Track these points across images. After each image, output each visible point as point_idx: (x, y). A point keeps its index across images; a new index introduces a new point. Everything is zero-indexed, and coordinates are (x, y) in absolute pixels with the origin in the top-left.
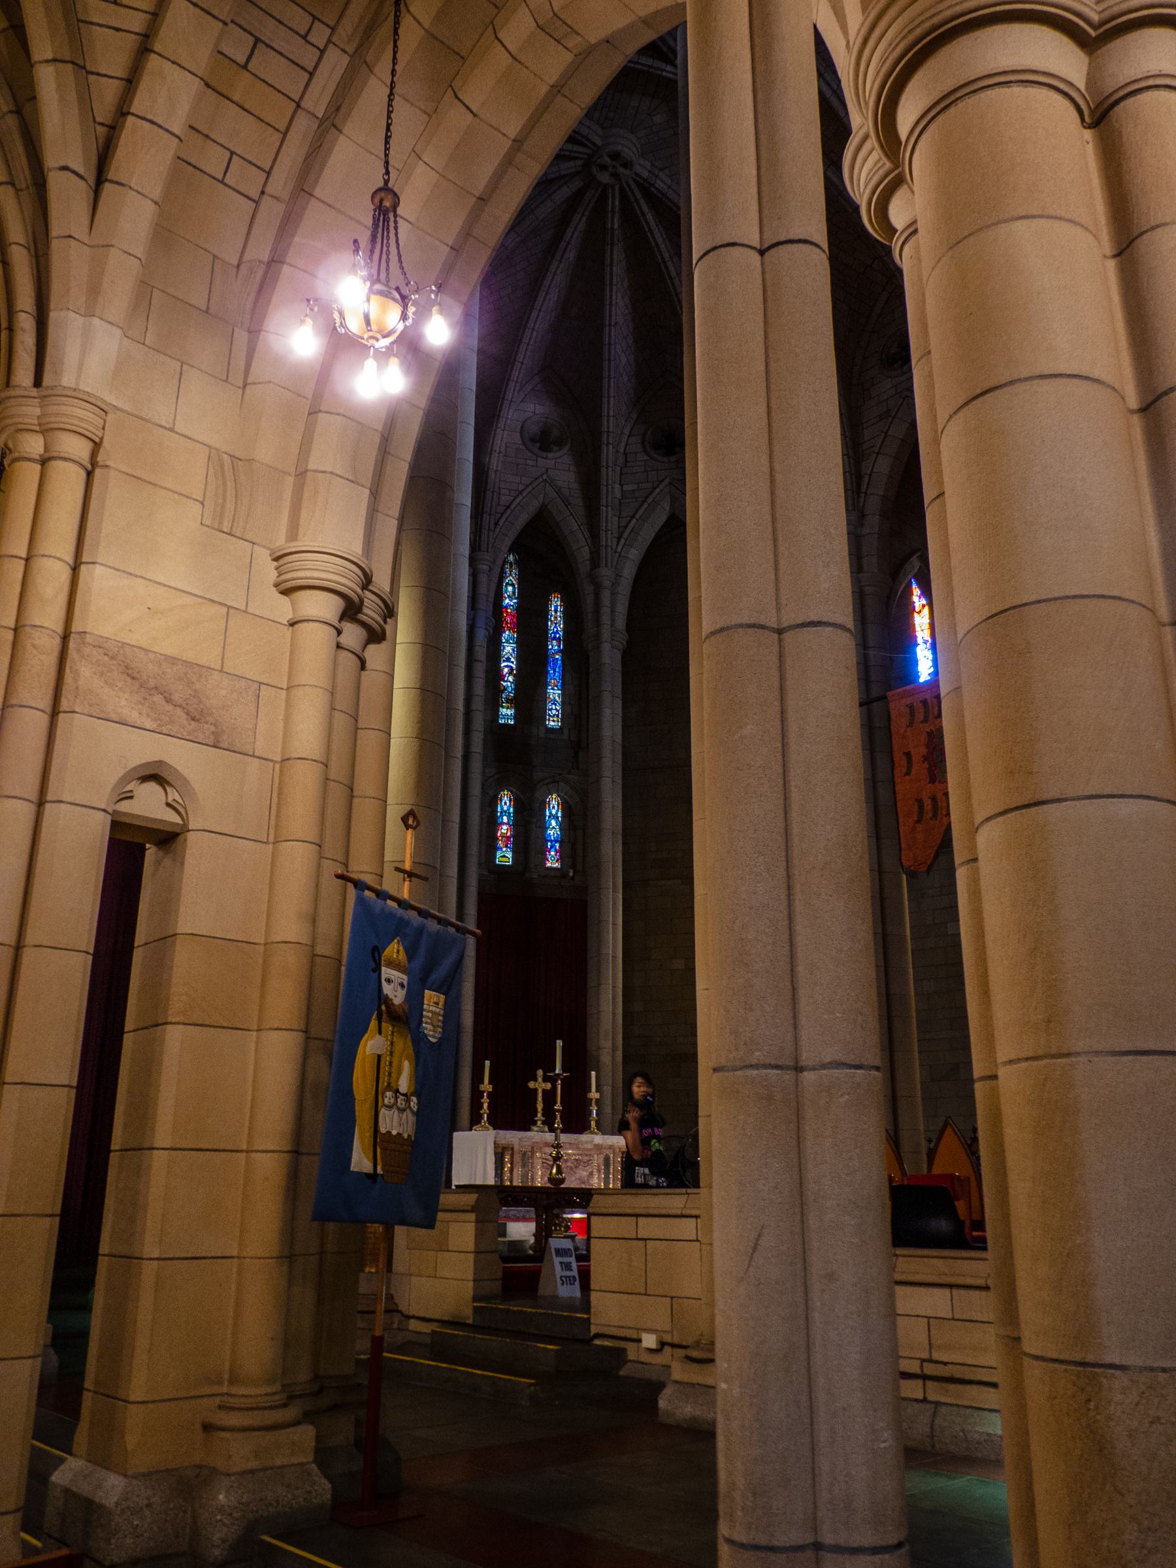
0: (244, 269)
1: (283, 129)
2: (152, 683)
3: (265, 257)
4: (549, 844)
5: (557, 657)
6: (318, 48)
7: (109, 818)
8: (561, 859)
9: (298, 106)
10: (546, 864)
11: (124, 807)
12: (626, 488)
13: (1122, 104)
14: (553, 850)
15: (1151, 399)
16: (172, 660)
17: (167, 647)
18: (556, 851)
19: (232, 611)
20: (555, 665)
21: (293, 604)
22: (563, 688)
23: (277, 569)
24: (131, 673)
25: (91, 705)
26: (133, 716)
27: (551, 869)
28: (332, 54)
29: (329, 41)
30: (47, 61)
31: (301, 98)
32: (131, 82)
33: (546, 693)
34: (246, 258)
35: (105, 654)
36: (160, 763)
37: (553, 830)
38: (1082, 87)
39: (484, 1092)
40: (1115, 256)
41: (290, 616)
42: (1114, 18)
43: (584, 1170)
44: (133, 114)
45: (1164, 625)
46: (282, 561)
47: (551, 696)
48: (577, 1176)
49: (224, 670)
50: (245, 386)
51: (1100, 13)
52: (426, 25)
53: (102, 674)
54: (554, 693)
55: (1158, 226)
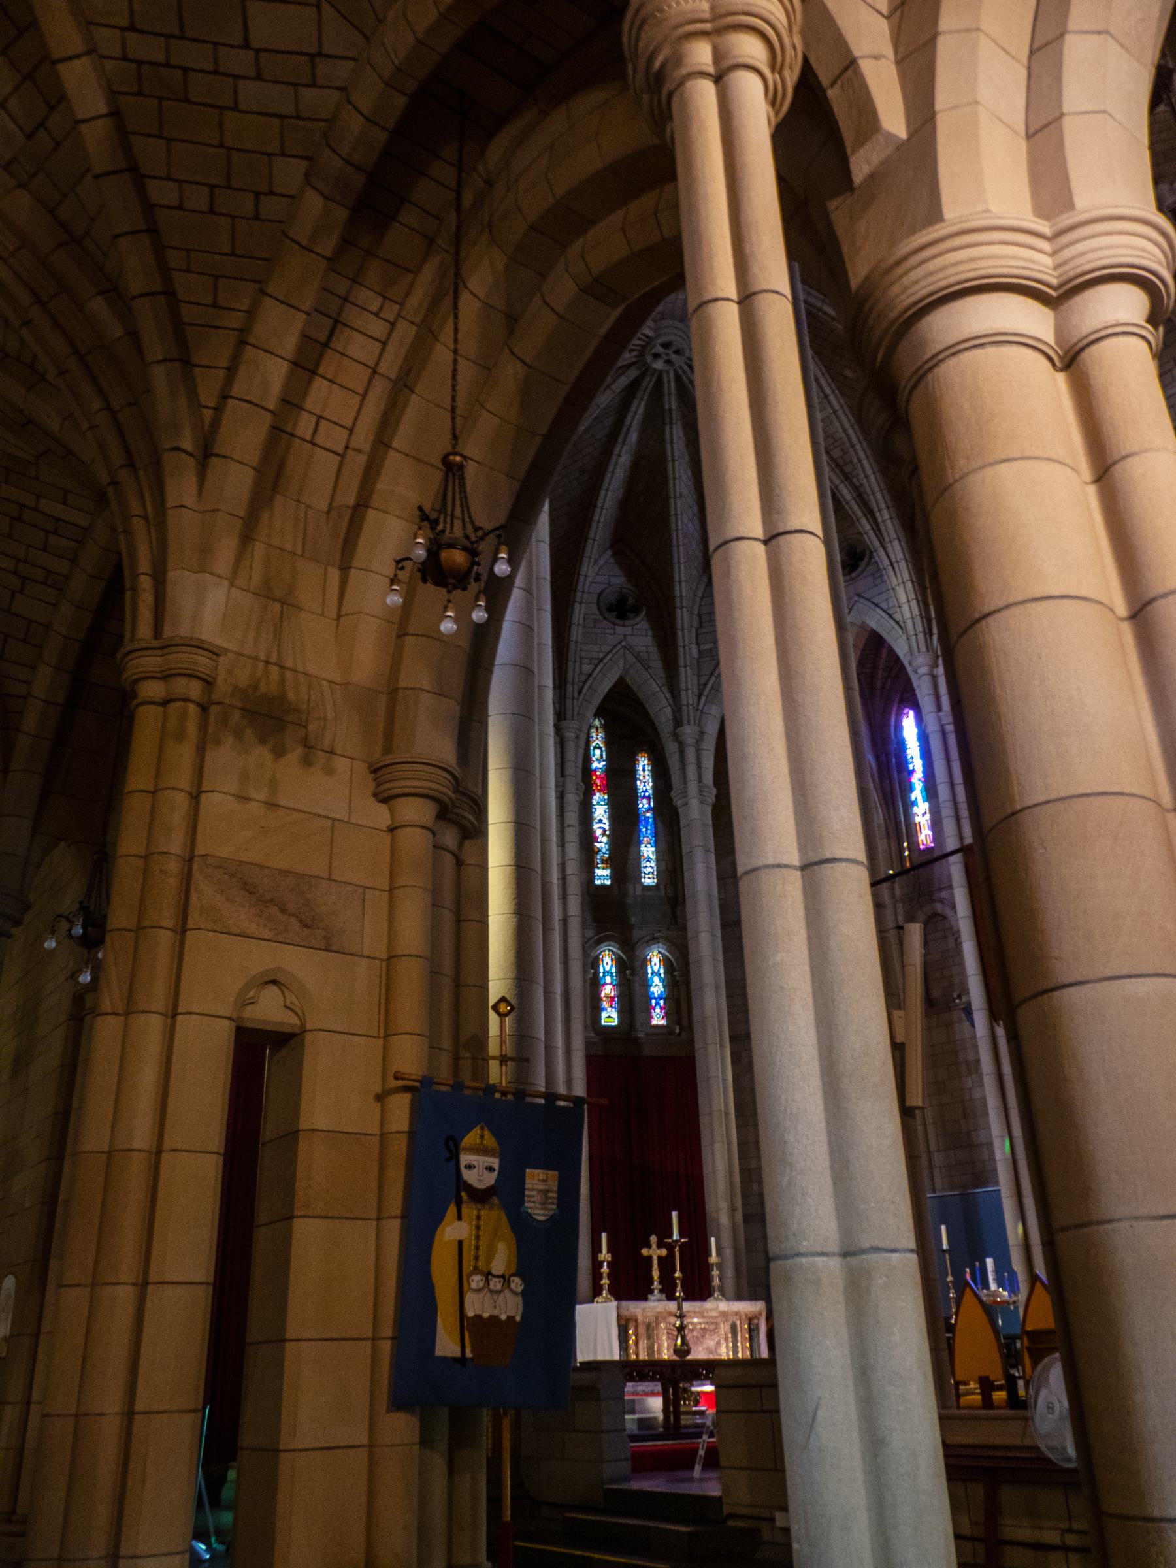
0: (334, 513)
1: (361, 390)
2: (268, 896)
3: (351, 501)
4: (653, 1002)
5: (648, 815)
6: (388, 321)
7: (233, 1025)
8: (666, 1016)
9: (375, 372)
10: (651, 1022)
11: (248, 1012)
12: (703, 647)
13: (1087, 351)
14: (657, 1007)
15: (1137, 609)
16: (285, 873)
18: (661, 1008)
19: (337, 823)
20: (647, 822)
21: (391, 811)
22: (656, 845)
23: (375, 780)
24: (248, 888)
26: (252, 928)
27: (657, 1026)
28: (402, 326)
29: (399, 315)
30: (158, 362)
31: (377, 363)
32: (231, 370)
33: (639, 851)
35: (225, 874)
37: (657, 988)
38: (1052, 342)
41: (389, 822)
42: (1070, 280)
43: (711, 1340)
45: (1168, 811)
47: (646, 855)
48: (705, 1346)
49: (332, 878)
51: (1057, 277)
52: (482, 295)
54: (648, 851)
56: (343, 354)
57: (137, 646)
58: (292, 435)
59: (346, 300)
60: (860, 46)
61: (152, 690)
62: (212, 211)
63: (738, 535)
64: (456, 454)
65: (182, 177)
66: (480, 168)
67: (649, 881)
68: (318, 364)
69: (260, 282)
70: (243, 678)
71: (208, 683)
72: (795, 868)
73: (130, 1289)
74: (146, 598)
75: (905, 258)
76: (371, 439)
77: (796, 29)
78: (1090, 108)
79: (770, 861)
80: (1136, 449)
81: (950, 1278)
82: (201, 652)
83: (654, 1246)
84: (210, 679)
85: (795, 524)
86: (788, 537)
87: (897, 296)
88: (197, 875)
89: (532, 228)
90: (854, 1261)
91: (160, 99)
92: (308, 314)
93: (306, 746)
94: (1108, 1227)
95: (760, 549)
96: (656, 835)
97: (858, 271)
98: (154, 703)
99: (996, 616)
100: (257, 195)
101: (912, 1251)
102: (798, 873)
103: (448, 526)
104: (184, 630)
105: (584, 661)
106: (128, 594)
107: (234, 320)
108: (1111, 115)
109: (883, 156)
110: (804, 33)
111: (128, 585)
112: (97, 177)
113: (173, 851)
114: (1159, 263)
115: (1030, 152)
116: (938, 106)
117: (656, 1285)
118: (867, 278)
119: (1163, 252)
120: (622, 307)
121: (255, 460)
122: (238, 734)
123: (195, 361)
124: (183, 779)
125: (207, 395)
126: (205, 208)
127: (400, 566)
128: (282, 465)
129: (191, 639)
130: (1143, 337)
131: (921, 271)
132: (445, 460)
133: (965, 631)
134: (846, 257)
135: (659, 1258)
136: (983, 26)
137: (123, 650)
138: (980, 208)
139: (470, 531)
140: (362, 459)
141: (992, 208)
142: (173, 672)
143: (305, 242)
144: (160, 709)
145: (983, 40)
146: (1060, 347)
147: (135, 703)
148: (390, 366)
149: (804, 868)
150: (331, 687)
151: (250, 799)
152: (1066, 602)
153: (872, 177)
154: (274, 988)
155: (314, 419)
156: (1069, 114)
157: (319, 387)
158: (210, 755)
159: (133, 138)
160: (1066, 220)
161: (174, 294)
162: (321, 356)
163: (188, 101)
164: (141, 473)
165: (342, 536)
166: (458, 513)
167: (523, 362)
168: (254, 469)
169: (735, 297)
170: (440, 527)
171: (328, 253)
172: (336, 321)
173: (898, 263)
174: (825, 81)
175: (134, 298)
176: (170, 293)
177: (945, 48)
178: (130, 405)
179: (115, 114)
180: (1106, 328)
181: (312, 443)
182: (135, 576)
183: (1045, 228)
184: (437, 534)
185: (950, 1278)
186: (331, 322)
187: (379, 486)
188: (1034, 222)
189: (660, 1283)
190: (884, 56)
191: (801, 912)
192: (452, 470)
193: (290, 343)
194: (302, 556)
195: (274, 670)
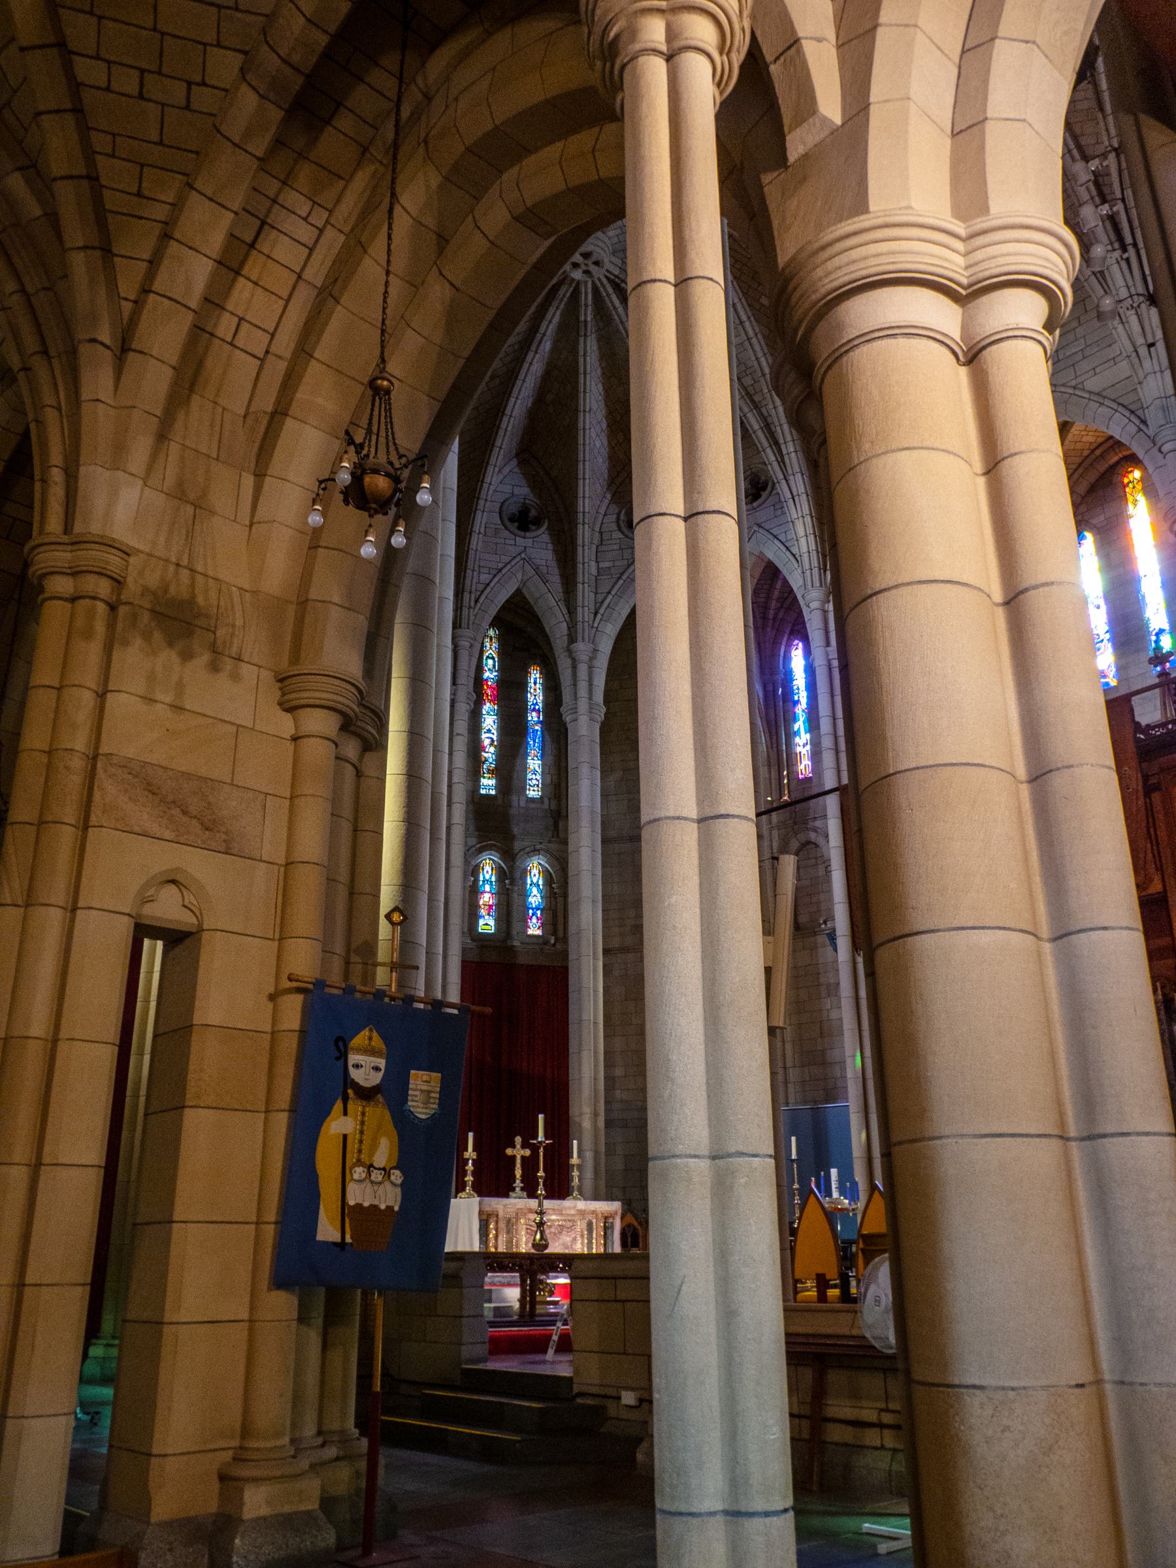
0: (249, 421)
1: (285, 295)
2: (170, 798)
3: (270, 409)
4: (531, 911)
5: (537, 728)
6: (317, 228)
7: (133, 921)
9: (300, 277)
10: (527, 931)
12: (602, 565)
13: (988, 349)
14: (534, 917)
15: (1012, 596)
16: (187, 776)
18: (538, 919)
19: (241, 729)
21: (296, 721)
23: (281, 689)
24: (151, 789)
25: (117, 820)
26: (155, 829)
28: (330, 233)
29: (327, 222)
30: (79, 248)
32: (154, 263)
36: (178, 869)
37: (535, 898)
40: (985, 474)
41: (293, 732)
42: (980, 282)
44: (154, 292)
45: (1022, 783)
46: (287, 682)
47: (531, 767)
51: (968, 277)
52: (414, 212)
53: (126, 791)
54: (534, 763)
55: (1016, 454)
56: (268, 257)
57: (47, 540)
58: (212, 335)
59: (274, 201)
60: (803, 28)
61: (61, 585)
62: (141, 96)
63: (662, 511)
64: (383, 379)
65: (113, 58)
66: (420, 81)
67: (533, 793)
68: (242, 263)
69: (188, 175)
70: (153, 580)
71: (118, 583)
72: (692, 820)
73: (24, 1169)
74: (57, 492)
75: (830, 244)
76: (292, 346)
77: (746, 13)
78: (1012, 116)
79: (671, 813)
80: (1023, 448)
81: (796, 1186)
82: (113, 551)
83: (518, 1146)
84: (120, 578)
85: (712, 505)
86: (706, 516)
87: (820, 279)
89: (468, 149)
92: (236, 213)
94: (938, 1142)
95: (680, 525)
96: (543, 748)
97: (786, 250)
98: (61, 598)
99: (886, 594)
100: (189, 84)
101: (770, 1156)
102: (696, 825)
103: (373, 450)
104: (95, 528)
105: (482, 570)
106: (38, 486)
107: (160, 212)
108: (1030, 125)
109: (818, 139)
110: (753, 17)
111: (37, 475)
113: (77, 748)
114: (1060, 273)
115: (954, 151)
116: (872, 99)
118: (793, 258)
119: (1065, 263)
120: (553, 239)
121: (174, 361)
122: (147, 637)
123: (115, 250)
124: (89, 676)
125: (128, 287)
126: (136, 93)
127: (323, 486)
128: (200, 364)
129: (102, 537)
130: (1040, 342)
131: (844, 258)
132: (372, 383)
134: (776, 233)
135: (523, 1158)
136: (920, 23)
137: (32, 543)
138: (904, 204)
139: (394, 458)
140: (282, 366)
141: (913, 205)
143: (237, 140)
144: (70, 605)
145: (920, 37)
147: (41, 597)
148: (317, 272)
149: (701, 821)
150: (241, 594)
151: (156, 701)
152: (949, 586)
153: (805, 157)
154: (173, 889)
155: (236, 320)
156: (991, 119)
158: (116, 655)
159: (61, 11)
160: (980, 224)
161: (97, 179)
162: (247, 255)
164: (55, 362)
166: (383, 433)
167: (451, 284)
168: (174, 368)
169: (672, 280)
170: (365, 452)
171: (259, 153)
172: (264, 223)
173: (823, 248)
174: (769, 58)
175: (55, 179)
176: (93, 178)
177: (884, 39)
178: (44, 289)
180: (1007, 330)
181: (231, 344)
182: (46, 468)
183: (960, 229)
184: (362, 459)
185: (796, 1186)
186: (258, 223)
187: (298, 395)
188: (950, 222)
189: (522, 1181)
190: (825, 39)
191: (696, 861)
192: (377, 392)
193: (216, 241)
194: (217, 459)
195: (185, 573)
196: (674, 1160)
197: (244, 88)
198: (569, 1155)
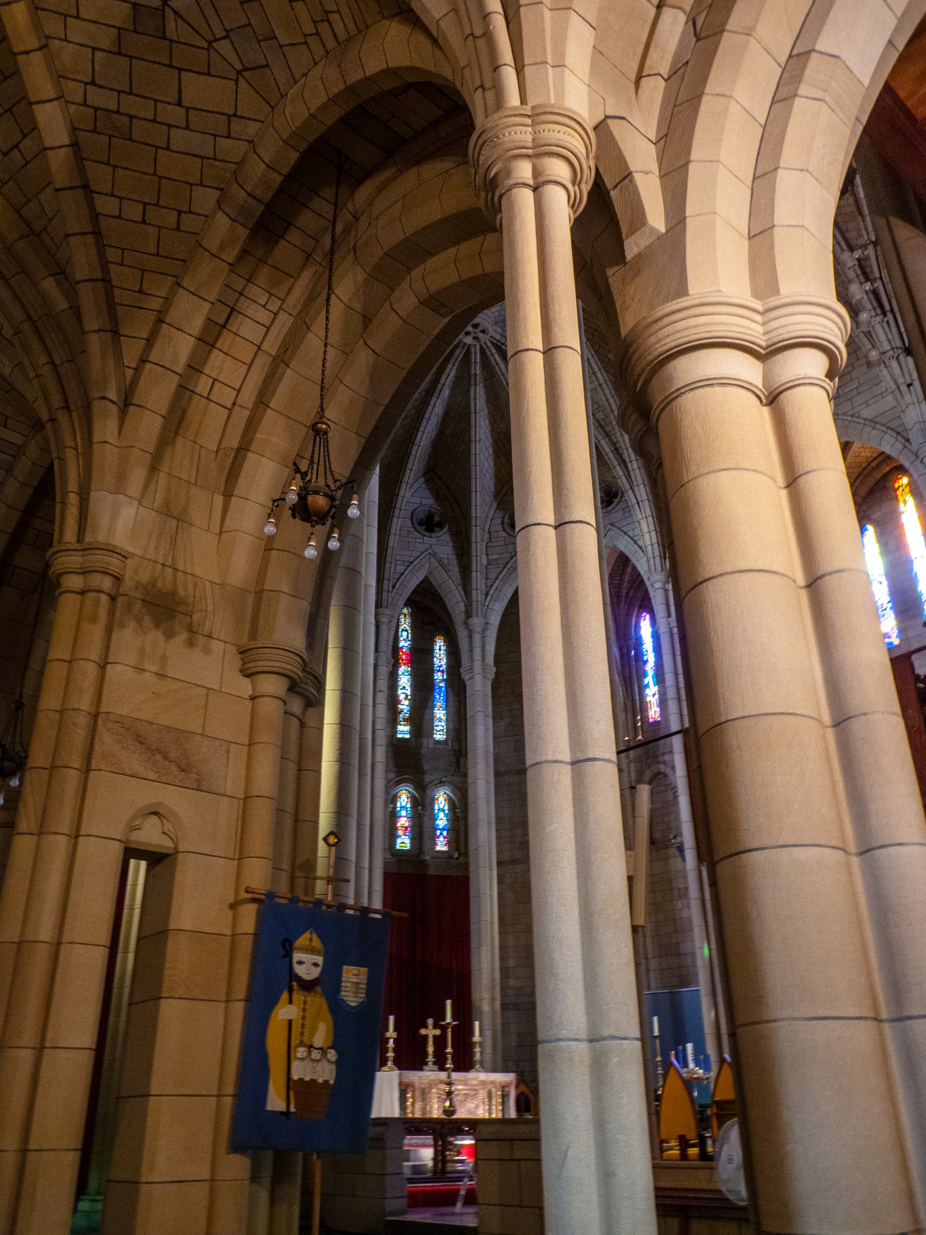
0: (221, 454)
1: (248, 362)
2: (155, 746)
3: (235, 445)
4: (438, 832)
5: (441, 685)
8: (448, 843)
9: (259, 348)
10: (434, 848)
12: (491, 557)
13: (784, 394)
15: (812, 580)
16: (169, 729)
17: (165, 720)
18: (445, 838)
20: (440, 691)
22: (447, 708)
23: (242, 659)
24: (140, 740)
25: (113, 764)
26: (141, 770)
27: (439, 852)
28: (282, 316)
29: (280, 307)
31: (262, 343)
32: (150, 341)
34: (223, 446)
36: (160, 803)
37: (442, 821)
38: (760, 386)
39: (389, 1038)
41: (250, 692)
42: (775, 344)
43: (472, 1103)
44: (150, 362)
46: (247, 654)
47: (438, 716)
48: (467, 1108)
49: (205, 734)
50: (220, 534)
51: (766, 341)
52: (345, 300)
54: (440, 713)
55: (809, 472)
57: (63, 548)
58: (193, 392)
59: (241, 294)
60: (634, 165)
61: (74, 582)
62: (144, 222)
63: (537, 522)
64: (323, 423)
66: (350, 205)
67: (439, 736)
69: (177, 277)
70: (144, 576)
71: (118, 579)
72: (567, 763)
74: (73, 511)
75: (660, 319)
76: (253, 399)
77: (591, 156)
78: (792, 223)
79: (550, 758)
80: (815, 467)
81: (659, 1059)
82: (115, 555)
84: (120, 577)
86: (572, 525)
87: (654, 345)
88: (101, 728)
89: (386, 254)
90: (597, 1045)
91: (110, 137)
92: (212, 303)
93: (190, 631)
95: (552, 532)
96: (447, 701)
97: (627, 323)
98: (73, 592)
99: (713, 581)
100: (179, 213)
101: (637, 1039)
102: (569, 767)
103: (314, 476)
104: (101, 538)
105: (398, 562)
106: (58, 506)
107: (155, 304)
108: (807, 229)
109: (648, 242)
110: (597, 158)
111: (58, 499)
112: (57, 190)
114: (836, 336)
115: (751, 249)
116: (687, 214)
117: (430, 1058)
118: (633, 329)
119: (839, 328)
120: (449, 318)
122: (139, 621)
123: (122, 331)
124: (94, 652)
125: (130, 358)
126: (140, 219)
127: (276, 504)
128: (184, 412)
129: (106, 545)
130: (823, 388)
131: (671, 329)
132: (314, 427)
133: (692, 589)
134: (619, 311)
135: (435, 1037)
136: (721, 160)
138: (715, 288)
139: (330, 482)
141: (722, 289)
142: (90, 569)
143: (214, 251)
144: (79, 597)
145: (721, 169)
146: (766, 390)
147: (59, 591)
148: (272, 345)
149: (574, 763)
150: (212, 587)
151: (144, 670)
152: (762, 574)
153: (639, 255)
154: (154, 819)
155: (211, 380)
156: (778, 226)
157: (216, 357)
158: (115, 635)
159: (85, 162)
160: (773, 302)
161: (110, 281)
162: (219, 334)
163: (131, 139)
164: (75, 415)
165: (227, 470)
166: (322, 463)
167: (374, 351)
168: (164, 417)
169: (541, 349)
170: (308, 478)
171: (231, 261)
172: (233, 310)
173: (655, 322)
174: (609, 186)
175: (78, 282)
177: (694, 171)
178: (68, 361)
179: (75, 145)
180: (798, 379)
181: (207, 398)
182: (65, 493)
183: (758, 305)
184: (306, 483)
185: (659, 1059)
187: (259, 435)
188: (751, 301)
189: (434, 1056)
190: (651, 172)
191: (570, 796)
192: (318, 433)
193: (197, 324)
194: (195, 484)
195: (169, 571)
196: (559, 1043)
197: (220, 214)
198: (471, 1033)
